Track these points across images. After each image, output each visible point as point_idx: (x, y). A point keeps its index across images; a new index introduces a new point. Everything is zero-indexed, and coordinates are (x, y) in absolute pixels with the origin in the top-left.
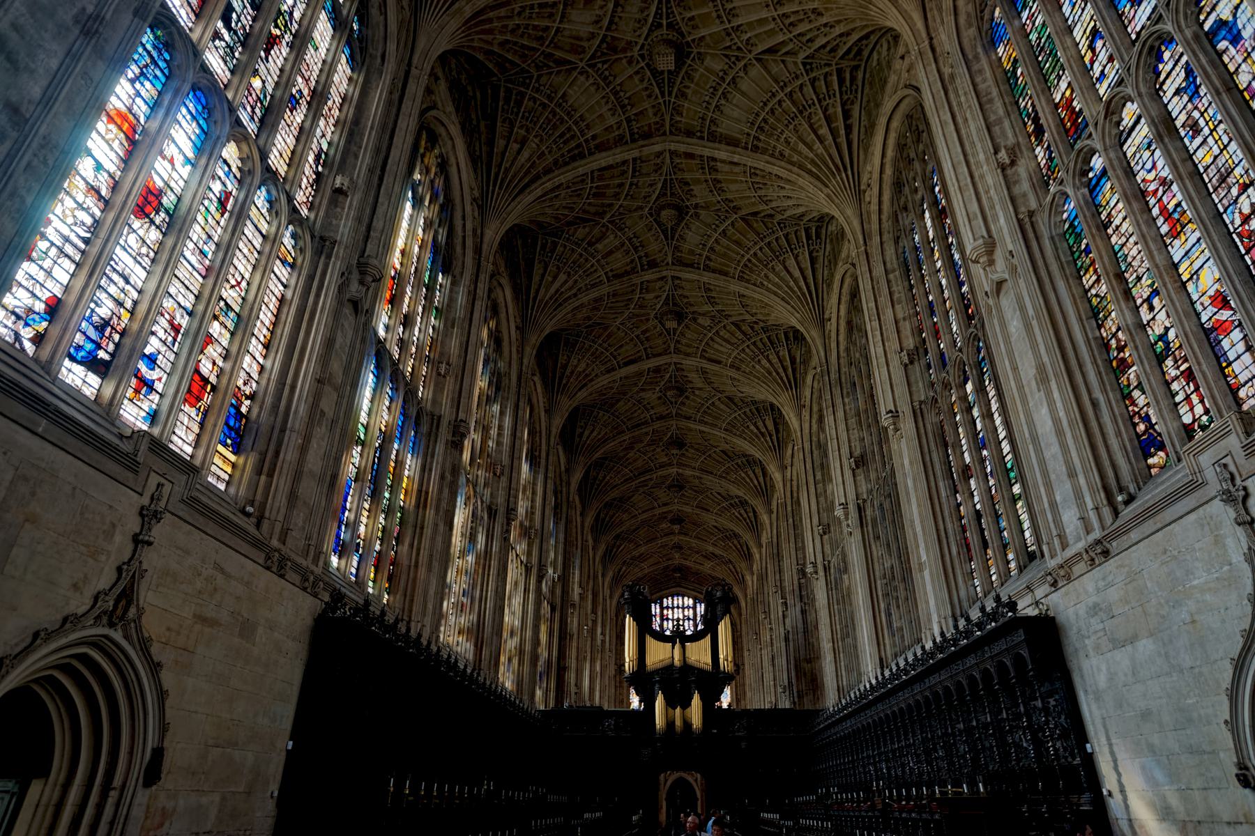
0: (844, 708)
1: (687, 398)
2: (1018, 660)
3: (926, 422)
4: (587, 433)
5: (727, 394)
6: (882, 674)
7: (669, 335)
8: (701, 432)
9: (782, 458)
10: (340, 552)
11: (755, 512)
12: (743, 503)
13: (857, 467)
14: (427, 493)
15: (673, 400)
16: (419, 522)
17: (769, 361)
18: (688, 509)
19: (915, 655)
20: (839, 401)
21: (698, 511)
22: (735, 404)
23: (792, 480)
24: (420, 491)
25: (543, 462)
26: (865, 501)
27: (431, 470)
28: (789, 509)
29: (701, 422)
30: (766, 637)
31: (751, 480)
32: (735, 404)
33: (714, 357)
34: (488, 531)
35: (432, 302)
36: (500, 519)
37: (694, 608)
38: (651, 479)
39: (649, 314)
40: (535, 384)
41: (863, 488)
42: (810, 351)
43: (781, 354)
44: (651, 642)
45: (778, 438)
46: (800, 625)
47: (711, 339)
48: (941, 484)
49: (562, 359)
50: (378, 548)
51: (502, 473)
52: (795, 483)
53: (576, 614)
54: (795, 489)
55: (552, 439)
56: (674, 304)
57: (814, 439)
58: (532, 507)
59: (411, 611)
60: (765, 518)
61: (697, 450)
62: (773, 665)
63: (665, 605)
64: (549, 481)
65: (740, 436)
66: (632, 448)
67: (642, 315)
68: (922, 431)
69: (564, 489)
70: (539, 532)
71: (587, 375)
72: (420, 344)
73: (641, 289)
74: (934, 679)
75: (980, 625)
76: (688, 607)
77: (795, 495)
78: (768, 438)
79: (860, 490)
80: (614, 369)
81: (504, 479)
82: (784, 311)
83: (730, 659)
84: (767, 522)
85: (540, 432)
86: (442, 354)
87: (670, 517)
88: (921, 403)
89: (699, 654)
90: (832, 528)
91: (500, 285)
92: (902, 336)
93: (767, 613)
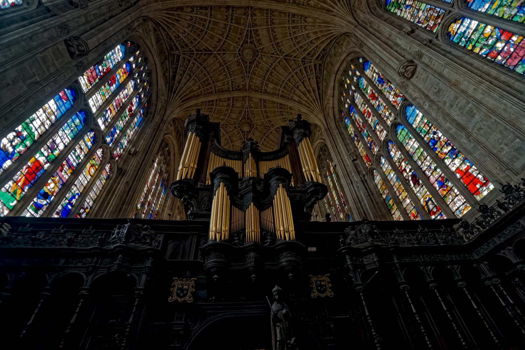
4: (184, 81)
23: (333, 108)
28: (333, 125)
46: (362, 194)
77: (337, 117)
78: (312, 94)
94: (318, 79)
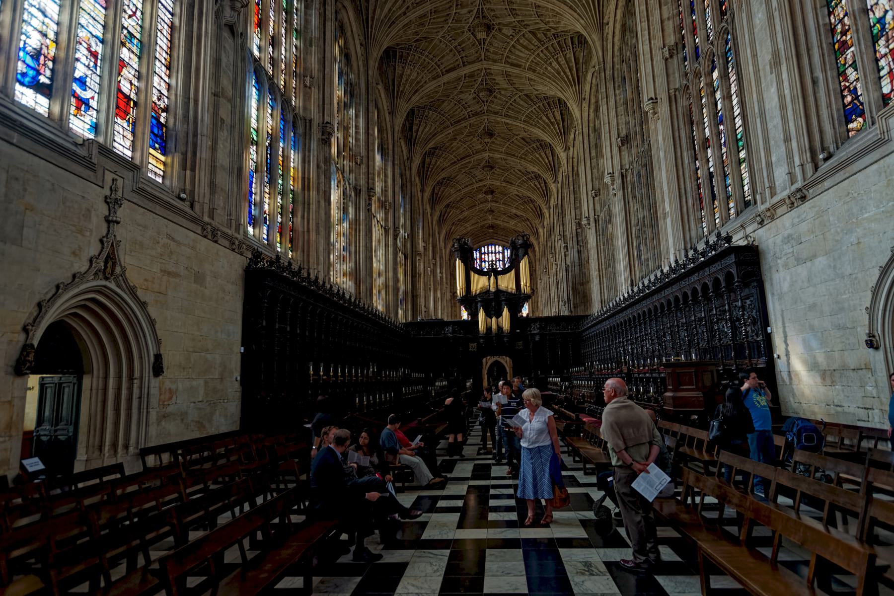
0: (605, 313)
1: (495, 97)
2: (729, 276)
3: (679, 105)
4: (421, 129)
5: (525, 92)
6: (632, 290)
7: (480, 44)
8: (506, 124)
9: (566, 141)
10: (254, 223)
11: (545, 183)
12: (537, 177)
13: (623, 145)
14: (309, 179)
15: (485, 99)
16: (306, 200)
17: (559, 63)
18: (497, 183)
19: (656, 276)
20: (611, 93)
21: (504, 184)
22: (532, 100)
23: (573, 158)
24: (303, 178)
25: (391, 152)
26: (627, 170)
27: (309, 162)
28: (571, 179)
29: (506, 116)
30: (552, 269)
31: (543, 159)
32: (532, 100)
33: (515, 62)
34: (356, 205)
35: (291, 24)
36: (364, 195)
37: (503, 253)
38: (470, 162)
39: (464, 28)
40: (379, 91)
41: (626, 161)
42: (590, 52)
43: (568, 56)
44: (474, 277)
45: (563, 126)
46: (577, 261)
47: (513, 46)
48: (685, 154)
49: (399, 70)
50: (279, 220)
51: (362, 162)
52: (575, 160)
53: (422, 260)
54: (575, 164)
55: (396, 135)
56: (483, 17)
57: (591, 125)
58: (385, 187)
59: (309, 262)
60: (553, 187)
61: (503, 138)
62: (558, 288)
63: (483, 251)
64: (396, 167)
65: (535, 126)
66: (455, 139)
67: (459, 28)
68: (675, 113)
69: (408, 173)
70: (392, 204)
71: (418, 83)
72: (288, 61)
73: (457, 5)
74: (667, 292)
75: (703, 254)
76: (499, 253)
77: (575, 169)
78: (556, 126)
79: (624, 163)
80: (438, 76)
81: (363, 166)
82: (571, 18)
83: (528, 285)
84: (555, 190)
85: (387, 129)
86: (305, 69)
87: (484, 190)
88: (676, 90)
89: (507, 283)
90: (602, 192)
91: (344, 7)
92: (666, 33)
93: (554, 254)
94: (563, 111)
